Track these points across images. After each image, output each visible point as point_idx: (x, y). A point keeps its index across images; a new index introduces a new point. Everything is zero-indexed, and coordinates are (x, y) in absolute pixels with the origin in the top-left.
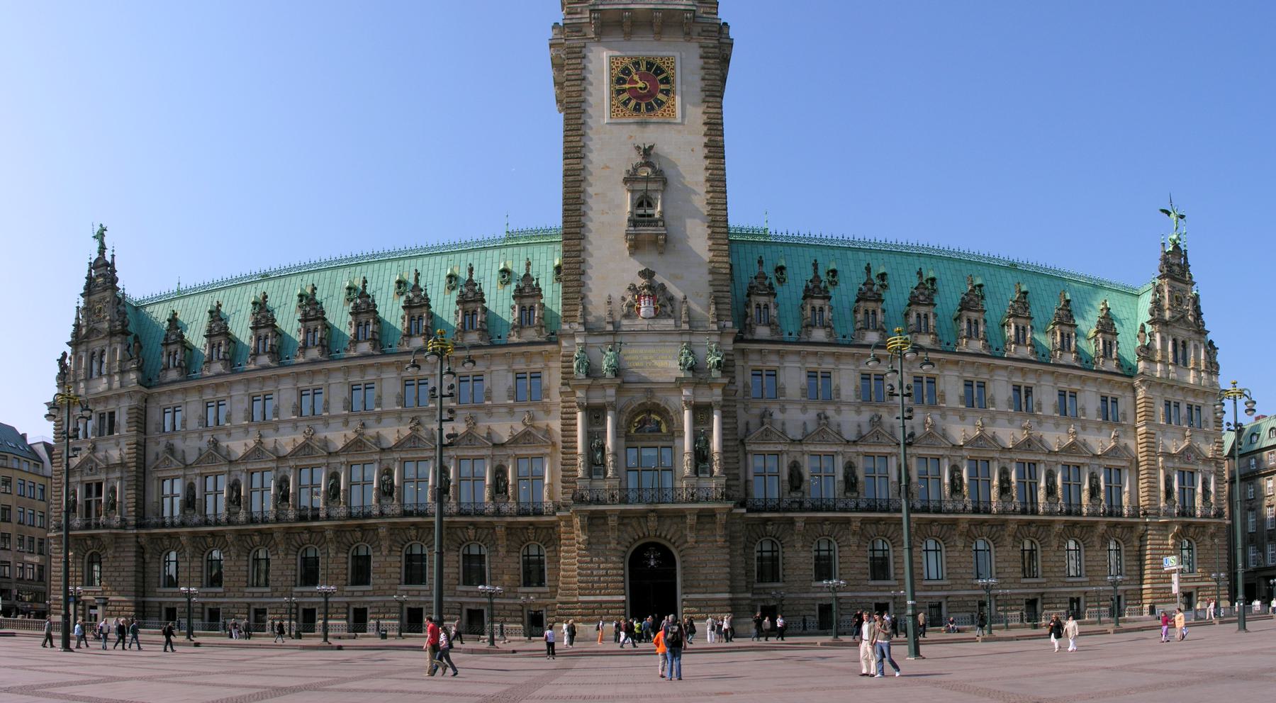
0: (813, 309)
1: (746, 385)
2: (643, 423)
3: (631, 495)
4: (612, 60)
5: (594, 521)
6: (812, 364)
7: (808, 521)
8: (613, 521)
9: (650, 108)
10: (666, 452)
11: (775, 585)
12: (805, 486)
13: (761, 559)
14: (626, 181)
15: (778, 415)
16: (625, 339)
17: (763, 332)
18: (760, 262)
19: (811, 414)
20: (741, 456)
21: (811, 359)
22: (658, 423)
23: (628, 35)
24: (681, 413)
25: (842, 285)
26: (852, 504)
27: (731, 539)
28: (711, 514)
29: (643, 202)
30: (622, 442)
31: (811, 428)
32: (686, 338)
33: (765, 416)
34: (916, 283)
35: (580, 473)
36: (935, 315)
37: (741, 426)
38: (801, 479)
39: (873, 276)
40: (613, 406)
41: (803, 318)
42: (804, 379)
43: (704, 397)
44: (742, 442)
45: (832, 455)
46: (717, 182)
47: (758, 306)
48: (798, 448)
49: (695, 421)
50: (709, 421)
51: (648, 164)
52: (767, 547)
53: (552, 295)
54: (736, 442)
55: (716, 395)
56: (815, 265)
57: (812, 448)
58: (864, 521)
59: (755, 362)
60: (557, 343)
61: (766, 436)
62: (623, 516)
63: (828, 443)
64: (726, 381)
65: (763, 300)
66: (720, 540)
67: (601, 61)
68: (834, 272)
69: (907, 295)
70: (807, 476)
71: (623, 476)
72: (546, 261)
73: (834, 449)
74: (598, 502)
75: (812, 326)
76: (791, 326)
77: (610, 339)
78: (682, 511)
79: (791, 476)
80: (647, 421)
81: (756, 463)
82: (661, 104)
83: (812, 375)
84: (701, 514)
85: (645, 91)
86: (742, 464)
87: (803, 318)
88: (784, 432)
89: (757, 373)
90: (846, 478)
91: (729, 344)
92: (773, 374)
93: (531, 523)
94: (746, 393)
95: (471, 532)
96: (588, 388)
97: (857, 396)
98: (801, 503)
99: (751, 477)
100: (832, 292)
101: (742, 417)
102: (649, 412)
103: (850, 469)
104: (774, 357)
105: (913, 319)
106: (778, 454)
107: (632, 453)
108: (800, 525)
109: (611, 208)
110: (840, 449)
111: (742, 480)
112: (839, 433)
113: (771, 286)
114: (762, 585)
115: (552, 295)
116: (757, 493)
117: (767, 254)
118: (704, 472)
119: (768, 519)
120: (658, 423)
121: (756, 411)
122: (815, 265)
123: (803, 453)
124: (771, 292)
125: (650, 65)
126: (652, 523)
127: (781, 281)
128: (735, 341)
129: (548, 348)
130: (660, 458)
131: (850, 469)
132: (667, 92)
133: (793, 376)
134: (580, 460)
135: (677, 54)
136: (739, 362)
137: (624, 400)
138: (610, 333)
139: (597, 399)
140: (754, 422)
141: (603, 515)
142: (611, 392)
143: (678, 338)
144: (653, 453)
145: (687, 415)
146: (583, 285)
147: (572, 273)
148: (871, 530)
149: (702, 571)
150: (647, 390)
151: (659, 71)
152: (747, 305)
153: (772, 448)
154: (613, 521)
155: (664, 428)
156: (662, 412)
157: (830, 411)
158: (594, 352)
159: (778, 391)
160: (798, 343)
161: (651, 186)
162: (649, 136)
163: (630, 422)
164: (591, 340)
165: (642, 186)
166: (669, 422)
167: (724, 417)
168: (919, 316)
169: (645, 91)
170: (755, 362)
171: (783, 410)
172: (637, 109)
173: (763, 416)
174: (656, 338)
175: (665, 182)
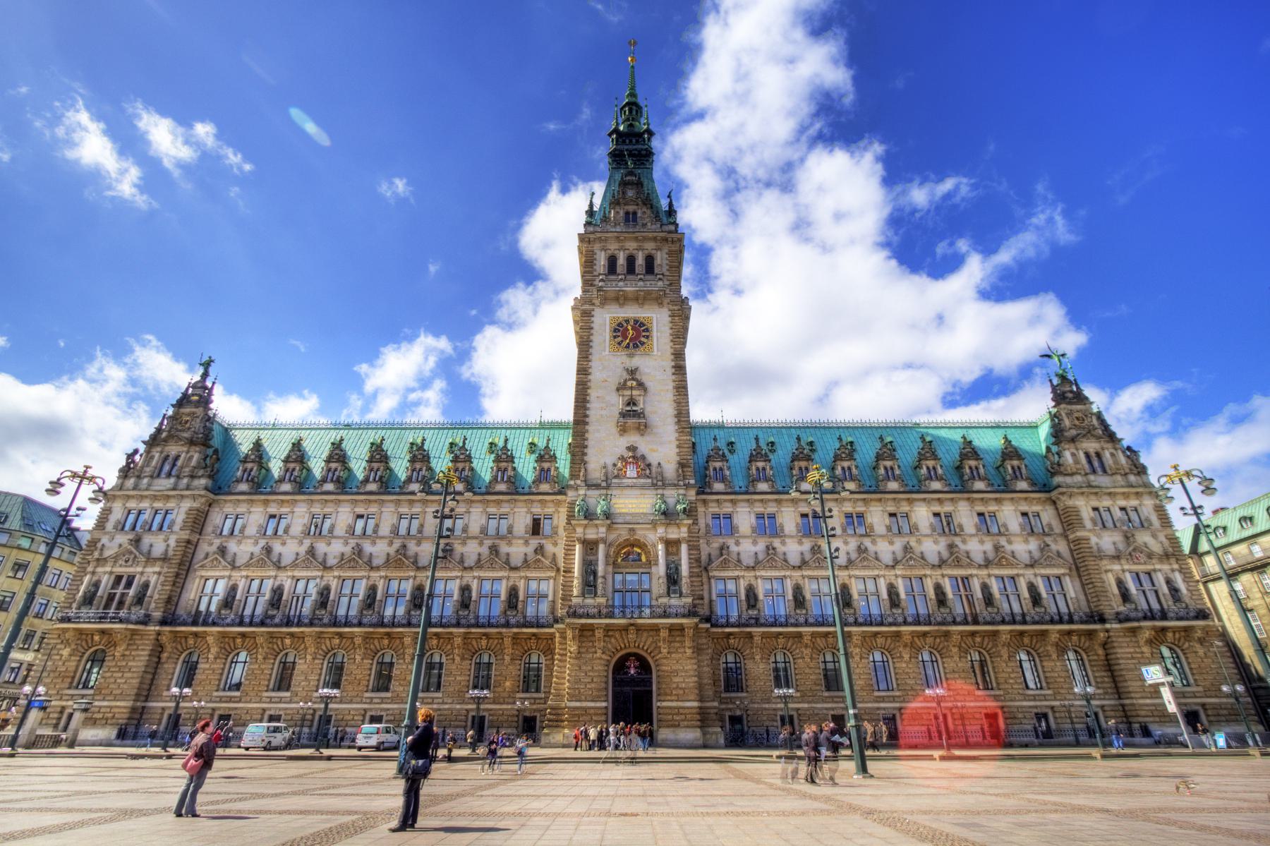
0: (758, 469)
1: (707, 525)
2: (628, 554)
3: (617, 611)
5: (585, 633)
6: (759, 508)
7: (764, 635)
8: (599, 634)
9: (636, 346)
10: (645, 577)
11: (740, 695)
12: (760, 605)
13: (727, 670)
14: (618, 390)
15: (734, 548)
16: (614, 492)
17: (718, 486)
18: (715, 439)
19: (761, 546)
20: (705, 580)
21: (758, 504)
22: (639, 554)
23: (622, 305)
24: (655, 546)
25: (780, 452)
26: (802, 620)
27: (698, 650)
28: (681, 628)
30: (610, 569)
31: (761, 557)
32: (660, 491)
33: (723, 549)
34: (837, 445)
35: (575, 592)
36: (857, 467)
37: (704, 558)
38: (756, 598)
39: (803, 443)
40: (604, 541)
41: (749, 476)
42: (753, 520)
43: (673, 534)
44: (706, 569)
45: (782, 579)
46: (681, 389)
47: (715, 469)
48: (752, 574)
49: (668, 553)
50: (678, 553)
51: (633, 379)
52: (731, 658)
53: (564, 465)
54: (702, 567)
55: (683, 533)
56: (757, 439)
57: (763, 573)
58: (813, 635)
59: (714, 509)
60: (565, 494)
61: (725, 565)
62: (608, 629)
63: (776, 568)
64: (690, 522)
65: (718, 465)
66: (689, 651)
67: (604, 318)
68: (773, 443)
69: (832, 455)
70: (761, 597)
71: (610, 596)
72: (561, 443)
73: (782, 573)
74: (588, 616)
75: (759, 480)
76: (739, 482)
77: (604, 492)
78: (656, 625)
79: (747, 596)
80: (630, 553)
81: (717, 587)
83: (760, 517)
84: (671, 629)
85: (632, 336)
86: (706, 587)
87: (749, 476)
88: (739, 561)
89: (716, 517)
90: (795, 597)
91: (692, 494)
92: (729, 517)
93: (534, 634)
94: (708, 532)
95: (484, 642)
96: (586, 526)
97: (799, 531)
98: (757, 619)
99: (714, 597)
100: (771, 457)
101: (705, 550)
102: (633, 546)
103: (798, 590)
104: (729, 505)
105: (839, 471)
106: (736, 579)
107: (619, 577)
108: (757, 639)
109: (606, 405)
110: (788, 573)
111: (706, 601)
112: (786, 560)
113: (724, 455)
114: (728, 695)
115: (564, 465)
116: (719, 610)
117: (720, 434)
118: (675, 592)
119: (730, 634)
120: (639, 554)
121: (716, 545)
122: (757, 439)
123: (756, 578)
124: (724, 458)
126: (632, 636)
127: (732, 452)
128: (698, 493)
129: (559, 497)
130: (640, 582)
131: (798, 590)
132: (647, 337)
133: (744, 518)
134: (576, 582)
136: (701, 509)
137: (612, 537)
138: (604, 488)
139: (591, 535)
140: (715, 553)
141: (591, 628)
142: (603, 530)
143: (652, 492)
144: (635, 578)
145: (660, 547)
146: (585, 454)
147: (578, 451)
148: (820, 642)
149: (676, 680)
150: (631, 530)
151: (642, 324)
152: (706, 468)
153: (730, 574)
154: (599, 634)
155: (644, 558)
156: (642, 546)
157: (776, 543)
158: (592, 501)
159: (733, 530)
160: (747, 493)
161: (635, 392)
163: (618, 554)
164: (590, 493)
165: (628, 393)
166: (648, 553)
167: (690, 548)
168: (843, 468)
169: (632, 336)
170: (714, 509)
171: (737, 543)
173: (721, 549)
174: (638, 492)
175: (645, 390)
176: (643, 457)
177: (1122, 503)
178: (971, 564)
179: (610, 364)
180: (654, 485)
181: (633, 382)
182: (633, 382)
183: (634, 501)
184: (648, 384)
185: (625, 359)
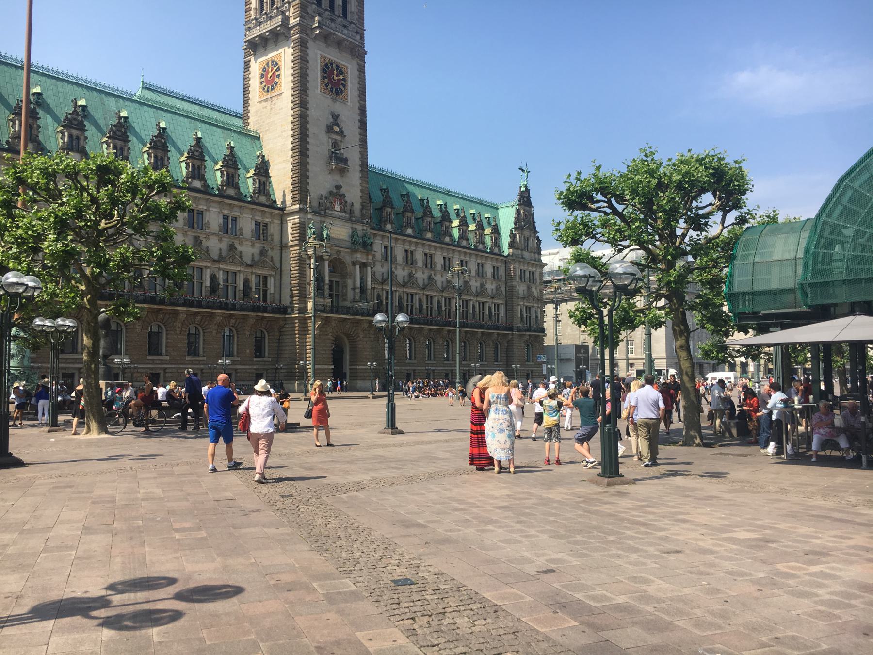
4: (322, 57)
9: (337, 93)
29: (335, 145)
77: (323, 219)
82: (342, 92)
109: (320, 145)
125: (337, 67)
135: (349, 66)
143: (349, 225)
150: (338, 251)
162: (338, 108)
172: (331, 91)
174: (341, 223)
176: (343, 196)
177: (530, 269)
178: (471, 295)
179: (321, 104)
180: (350, 220)
181: (334, 126)
182: (334, 126)
183: (339, 229)
184: (346, 133)
185: (329, 102)
